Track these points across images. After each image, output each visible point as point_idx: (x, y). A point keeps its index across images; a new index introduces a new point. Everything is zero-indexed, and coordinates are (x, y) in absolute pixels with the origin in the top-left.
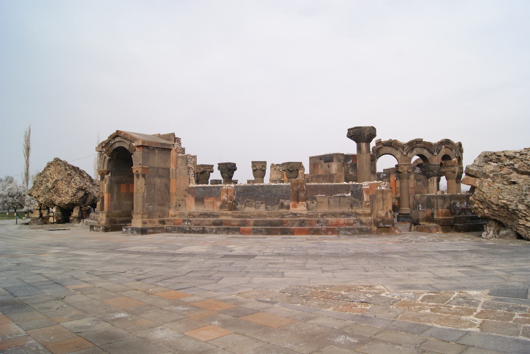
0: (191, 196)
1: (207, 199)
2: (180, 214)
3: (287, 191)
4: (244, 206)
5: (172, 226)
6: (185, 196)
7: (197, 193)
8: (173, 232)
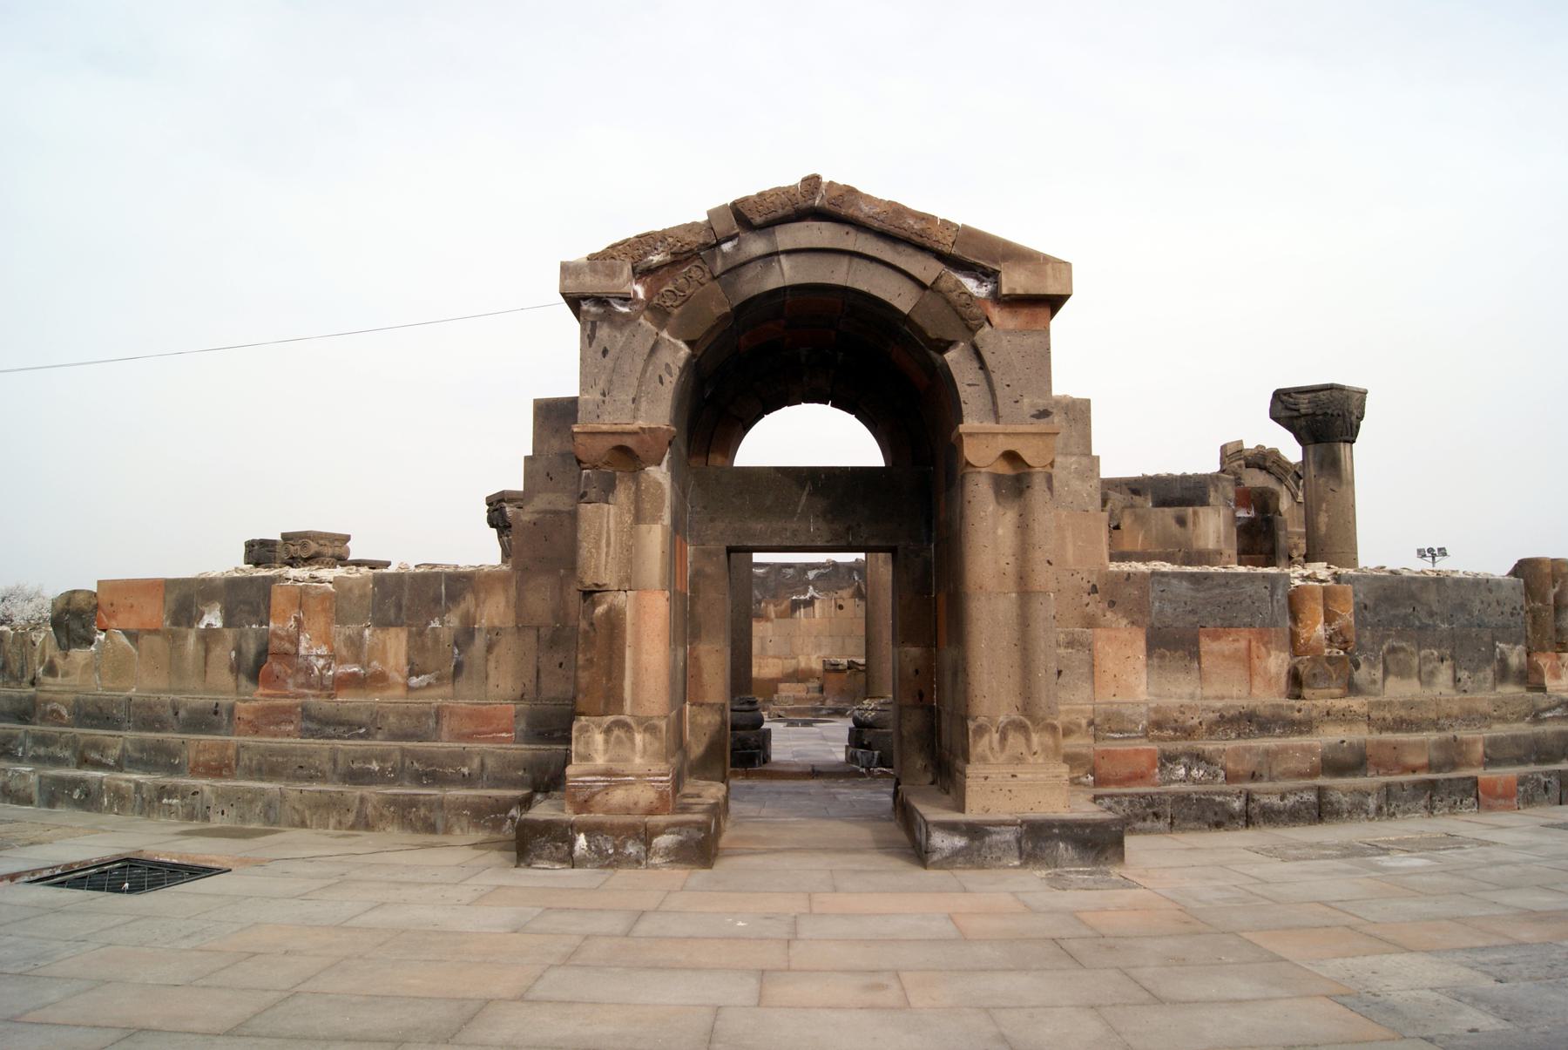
0: (1124, 622)
1: (1216, 637)
2: (1098, 721)
3: (1515, 608)
4: (1381, 671)
5: (1132, 795)
6: (1091, 622)
7: (1157, 604)
8: (1139, 825)
